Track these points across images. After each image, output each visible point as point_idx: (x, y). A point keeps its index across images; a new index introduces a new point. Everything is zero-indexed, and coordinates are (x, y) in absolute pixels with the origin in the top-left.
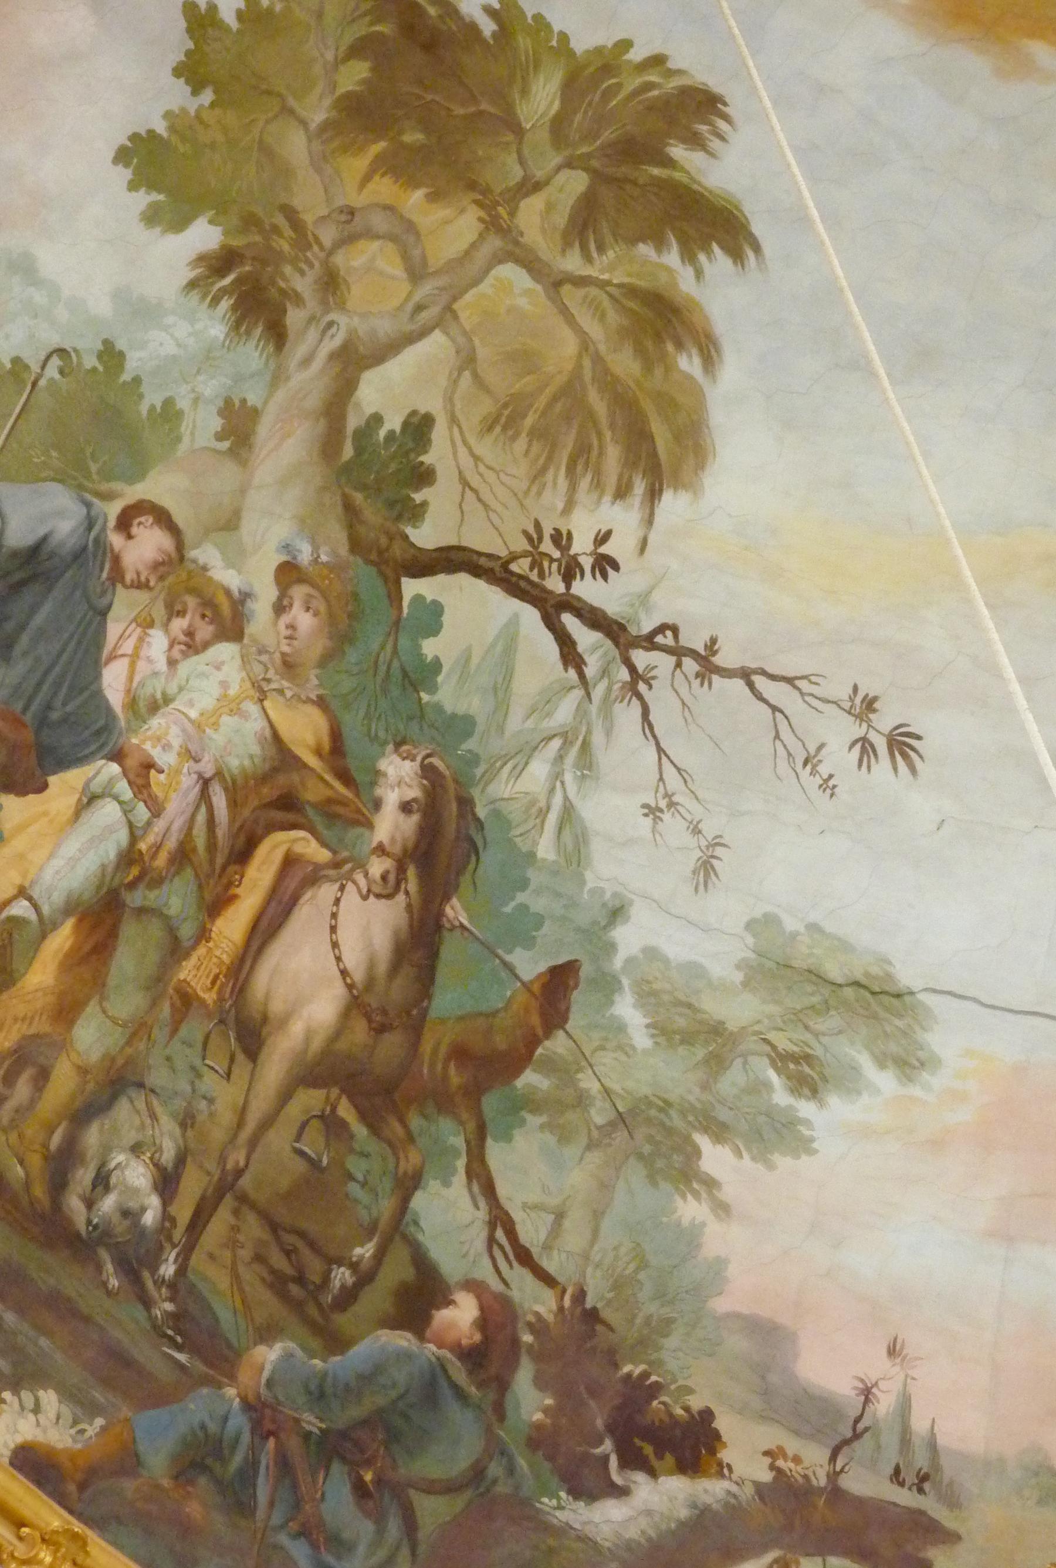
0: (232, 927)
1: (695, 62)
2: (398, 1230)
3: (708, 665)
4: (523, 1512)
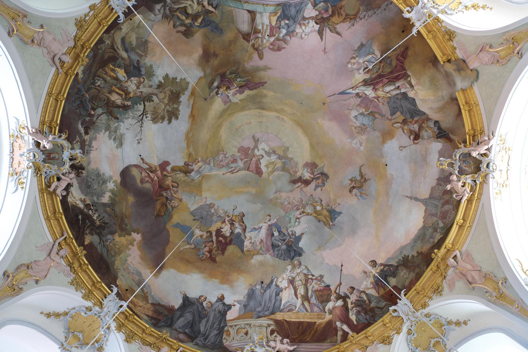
0: (117, 90)
1: (180, 117)
2: (98, 107)
3: (141, 127)
4: (79, 119)
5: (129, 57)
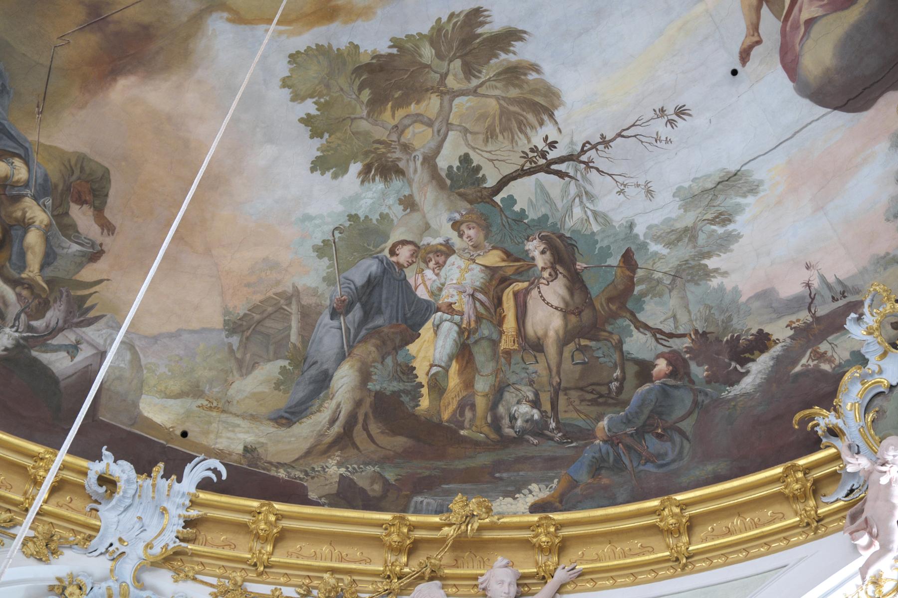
0: (510, 324)
2: (625, 359)
3: (605, 142)
4: (718, 402)
5: (342, 357)
